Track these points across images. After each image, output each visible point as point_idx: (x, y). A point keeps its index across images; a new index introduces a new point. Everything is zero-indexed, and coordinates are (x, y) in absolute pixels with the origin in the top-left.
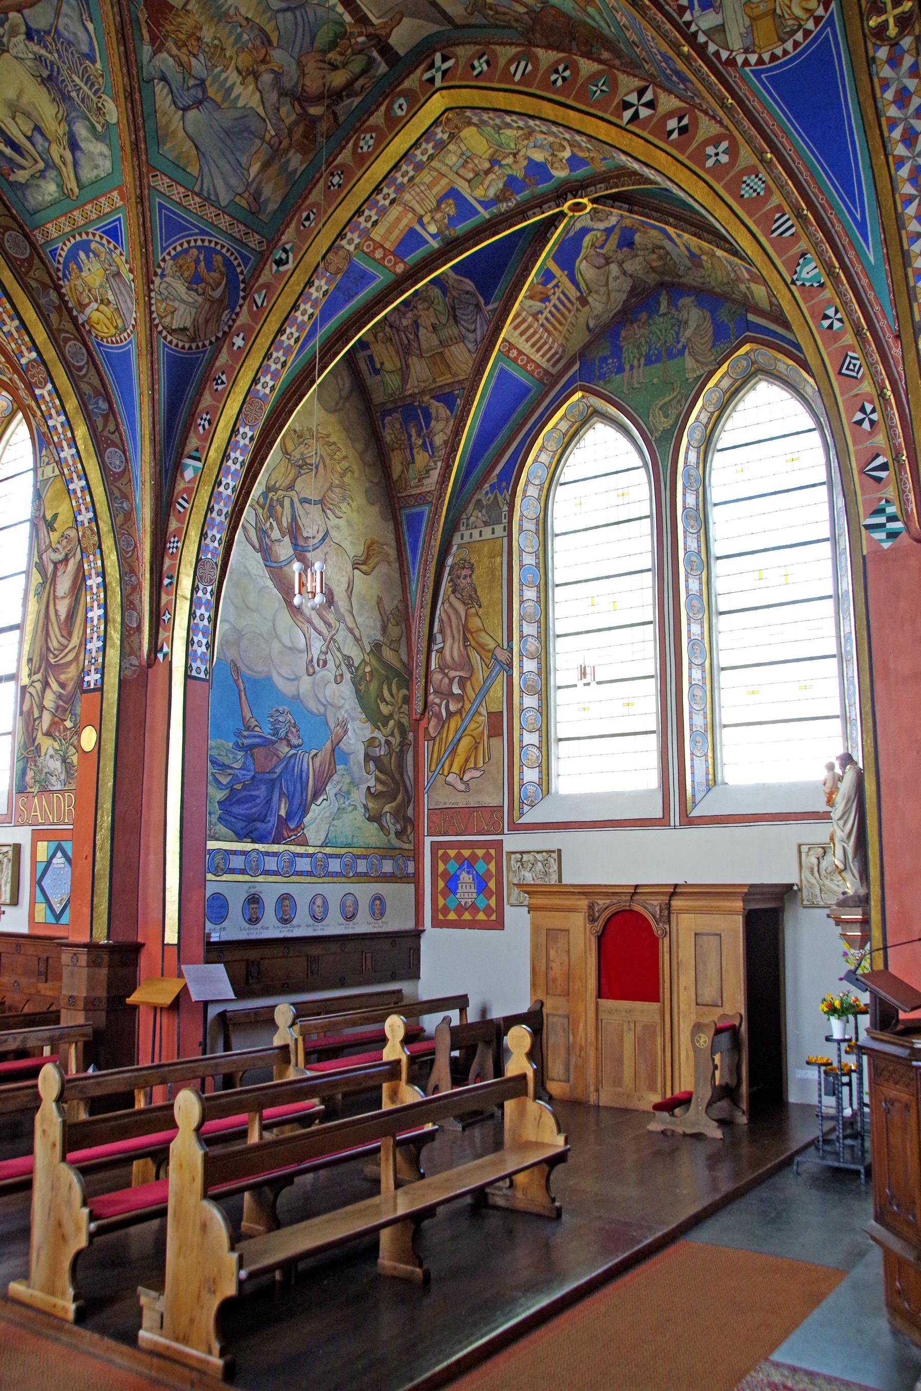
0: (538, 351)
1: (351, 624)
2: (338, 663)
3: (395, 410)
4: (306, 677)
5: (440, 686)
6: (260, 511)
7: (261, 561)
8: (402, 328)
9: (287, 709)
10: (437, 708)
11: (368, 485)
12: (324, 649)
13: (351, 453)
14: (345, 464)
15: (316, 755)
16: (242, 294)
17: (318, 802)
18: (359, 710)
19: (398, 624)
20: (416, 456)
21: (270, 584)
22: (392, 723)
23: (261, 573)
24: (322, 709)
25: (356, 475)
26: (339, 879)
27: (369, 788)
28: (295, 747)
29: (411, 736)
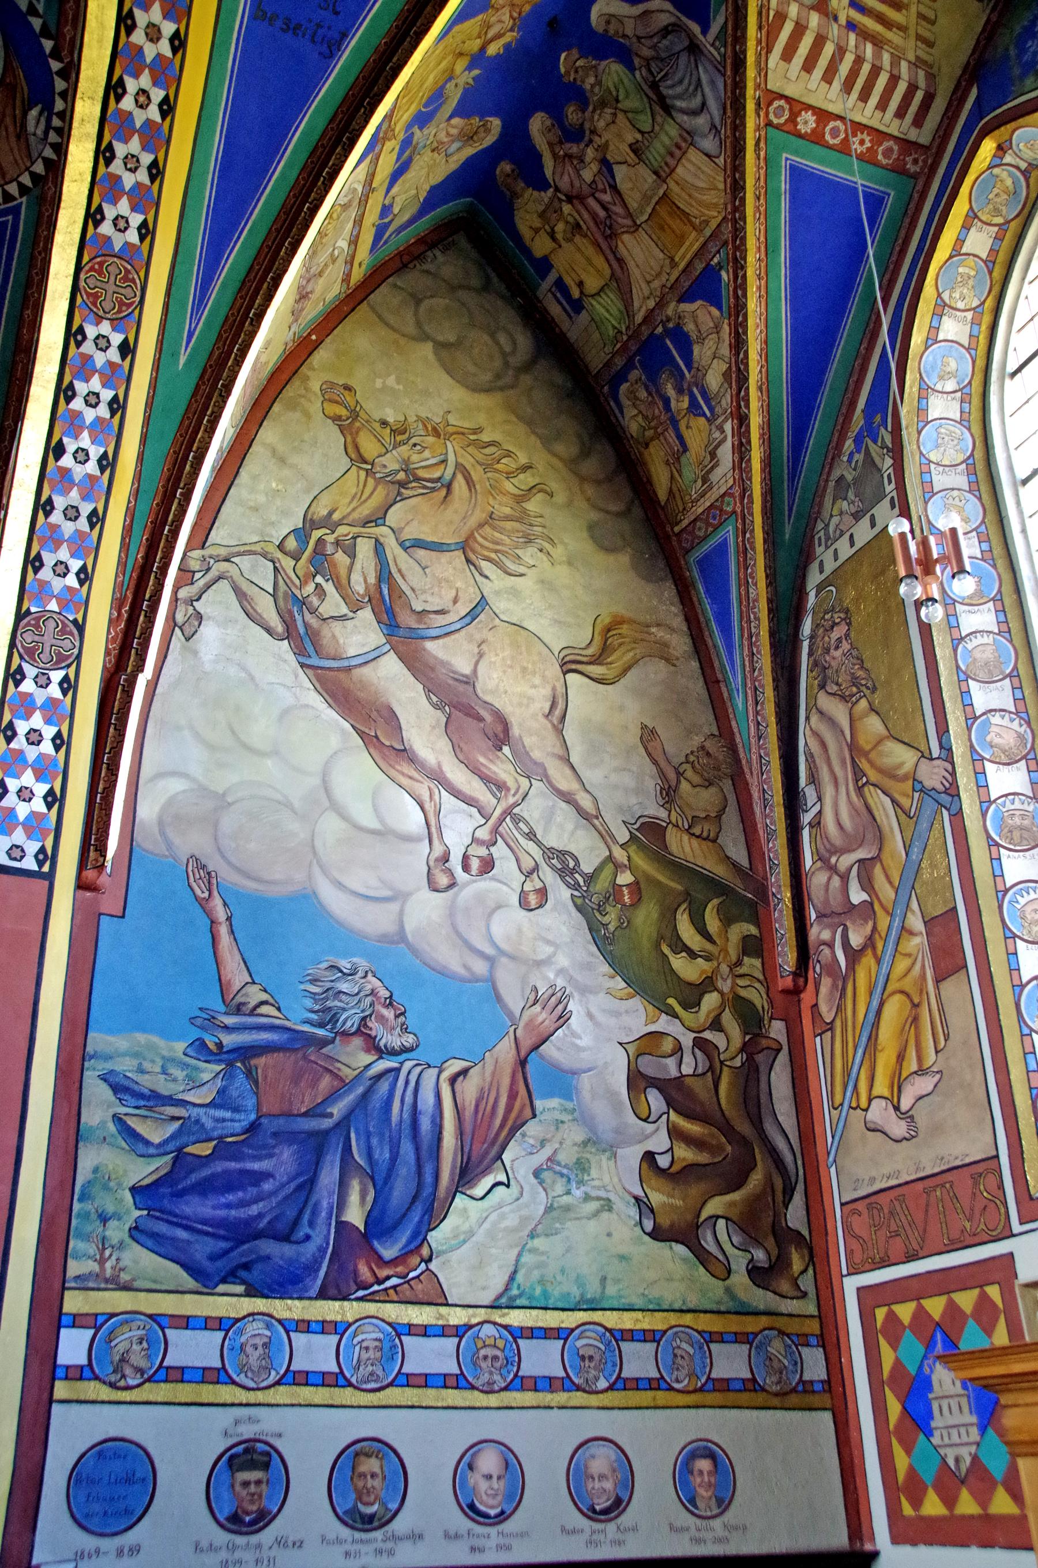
0: (864, 96)
1: (565, 782)
2: (528, 864)
3: (629, 366)
4: (426, 894)
5: (827, 901)
6: (288, 563)
7: (291, 657)
8: (586, 190)
9: (363, 964)
10: (827, 951)
11: (594, 516)
12: (483, 834)
13: (541, 459)
14: (527, 480)
15: (464, 1072)
16: (55, 66)
17: (479, 1190)
18: (606, 968)
19: (709, 784)
20: (686, 434)
21: (315, 700)
22: (710, 1001)
23: (289, 680)
24: (480, 967)
25: (560, 498)
26: (561, 1397)
27: (649, 1157)
28: (393, 1053)
29: (777, 1030)
